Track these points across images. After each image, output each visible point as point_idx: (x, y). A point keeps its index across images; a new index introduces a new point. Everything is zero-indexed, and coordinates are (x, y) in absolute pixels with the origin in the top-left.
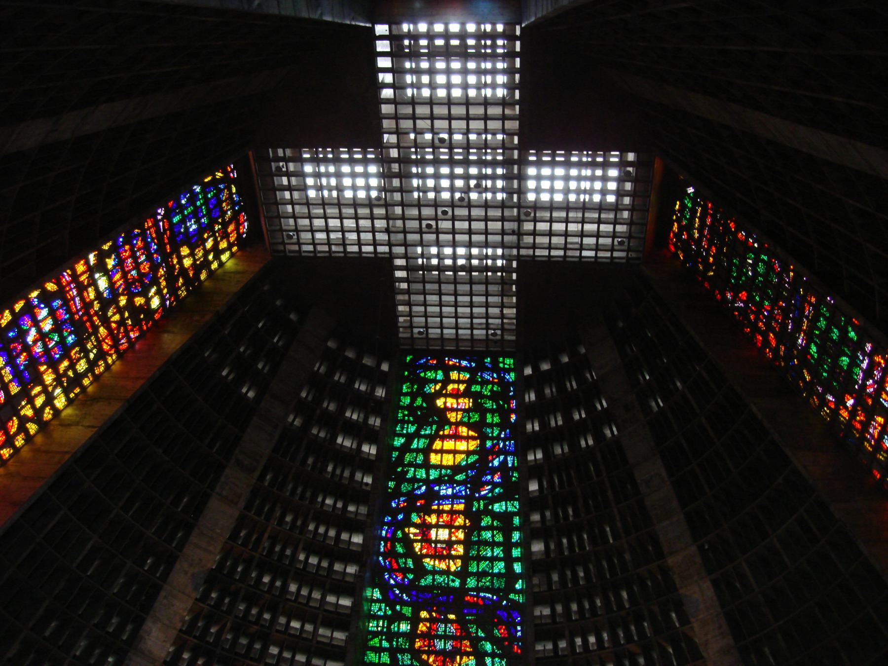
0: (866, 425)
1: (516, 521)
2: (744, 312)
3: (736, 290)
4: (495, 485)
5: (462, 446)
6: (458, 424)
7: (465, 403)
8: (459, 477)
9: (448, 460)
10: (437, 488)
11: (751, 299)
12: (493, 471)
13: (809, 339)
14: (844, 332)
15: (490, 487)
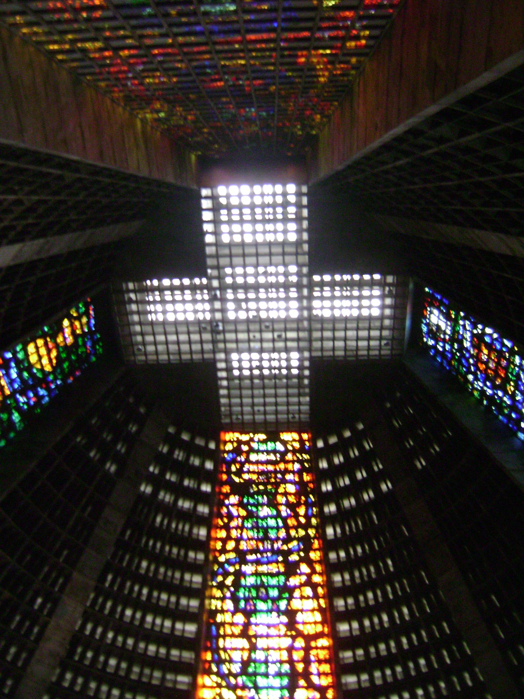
0: (233, 635)
1: (12, 435)
2: (230, 517)
3: (241, 504)
4: (28, 403)
5: (45, 361)
6: (57, 346)
7: (70, 340)
8: (26, 374)
9: (33, 359)
10: (13, 364)
11: (244, 518)
12: (36, 394)
13: (257, 574)
14: (280, 598)
15: (26, 400)
